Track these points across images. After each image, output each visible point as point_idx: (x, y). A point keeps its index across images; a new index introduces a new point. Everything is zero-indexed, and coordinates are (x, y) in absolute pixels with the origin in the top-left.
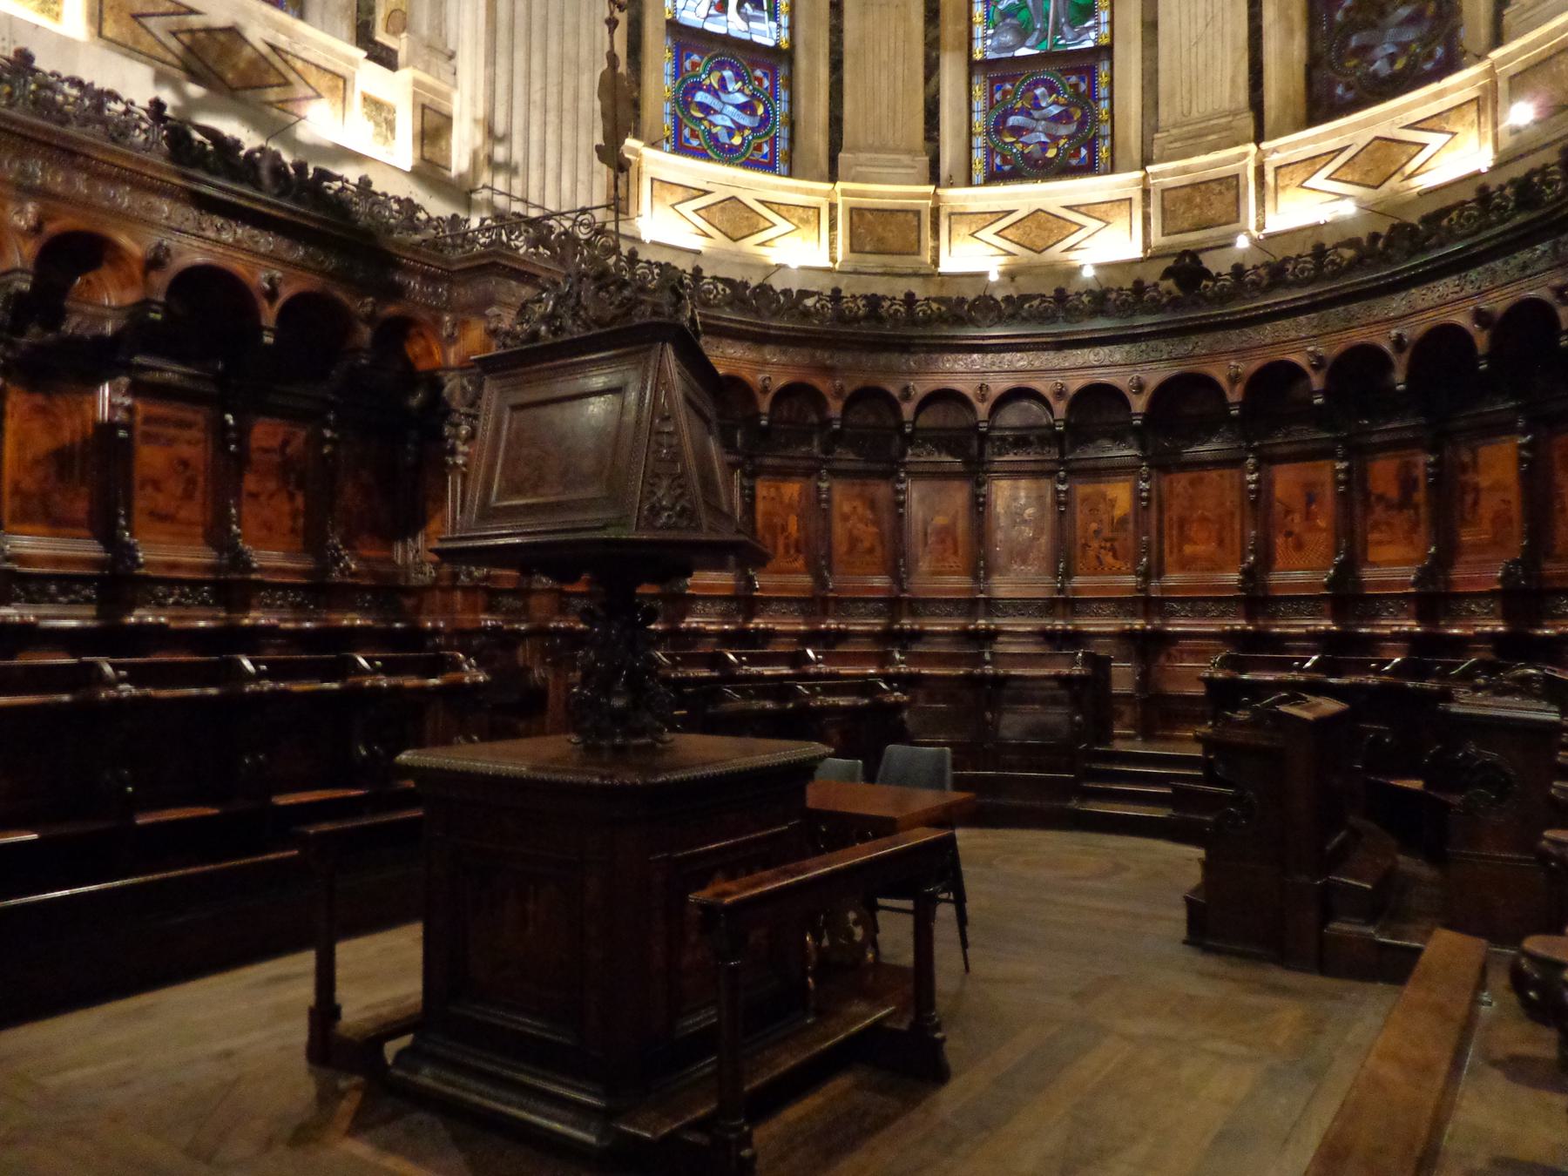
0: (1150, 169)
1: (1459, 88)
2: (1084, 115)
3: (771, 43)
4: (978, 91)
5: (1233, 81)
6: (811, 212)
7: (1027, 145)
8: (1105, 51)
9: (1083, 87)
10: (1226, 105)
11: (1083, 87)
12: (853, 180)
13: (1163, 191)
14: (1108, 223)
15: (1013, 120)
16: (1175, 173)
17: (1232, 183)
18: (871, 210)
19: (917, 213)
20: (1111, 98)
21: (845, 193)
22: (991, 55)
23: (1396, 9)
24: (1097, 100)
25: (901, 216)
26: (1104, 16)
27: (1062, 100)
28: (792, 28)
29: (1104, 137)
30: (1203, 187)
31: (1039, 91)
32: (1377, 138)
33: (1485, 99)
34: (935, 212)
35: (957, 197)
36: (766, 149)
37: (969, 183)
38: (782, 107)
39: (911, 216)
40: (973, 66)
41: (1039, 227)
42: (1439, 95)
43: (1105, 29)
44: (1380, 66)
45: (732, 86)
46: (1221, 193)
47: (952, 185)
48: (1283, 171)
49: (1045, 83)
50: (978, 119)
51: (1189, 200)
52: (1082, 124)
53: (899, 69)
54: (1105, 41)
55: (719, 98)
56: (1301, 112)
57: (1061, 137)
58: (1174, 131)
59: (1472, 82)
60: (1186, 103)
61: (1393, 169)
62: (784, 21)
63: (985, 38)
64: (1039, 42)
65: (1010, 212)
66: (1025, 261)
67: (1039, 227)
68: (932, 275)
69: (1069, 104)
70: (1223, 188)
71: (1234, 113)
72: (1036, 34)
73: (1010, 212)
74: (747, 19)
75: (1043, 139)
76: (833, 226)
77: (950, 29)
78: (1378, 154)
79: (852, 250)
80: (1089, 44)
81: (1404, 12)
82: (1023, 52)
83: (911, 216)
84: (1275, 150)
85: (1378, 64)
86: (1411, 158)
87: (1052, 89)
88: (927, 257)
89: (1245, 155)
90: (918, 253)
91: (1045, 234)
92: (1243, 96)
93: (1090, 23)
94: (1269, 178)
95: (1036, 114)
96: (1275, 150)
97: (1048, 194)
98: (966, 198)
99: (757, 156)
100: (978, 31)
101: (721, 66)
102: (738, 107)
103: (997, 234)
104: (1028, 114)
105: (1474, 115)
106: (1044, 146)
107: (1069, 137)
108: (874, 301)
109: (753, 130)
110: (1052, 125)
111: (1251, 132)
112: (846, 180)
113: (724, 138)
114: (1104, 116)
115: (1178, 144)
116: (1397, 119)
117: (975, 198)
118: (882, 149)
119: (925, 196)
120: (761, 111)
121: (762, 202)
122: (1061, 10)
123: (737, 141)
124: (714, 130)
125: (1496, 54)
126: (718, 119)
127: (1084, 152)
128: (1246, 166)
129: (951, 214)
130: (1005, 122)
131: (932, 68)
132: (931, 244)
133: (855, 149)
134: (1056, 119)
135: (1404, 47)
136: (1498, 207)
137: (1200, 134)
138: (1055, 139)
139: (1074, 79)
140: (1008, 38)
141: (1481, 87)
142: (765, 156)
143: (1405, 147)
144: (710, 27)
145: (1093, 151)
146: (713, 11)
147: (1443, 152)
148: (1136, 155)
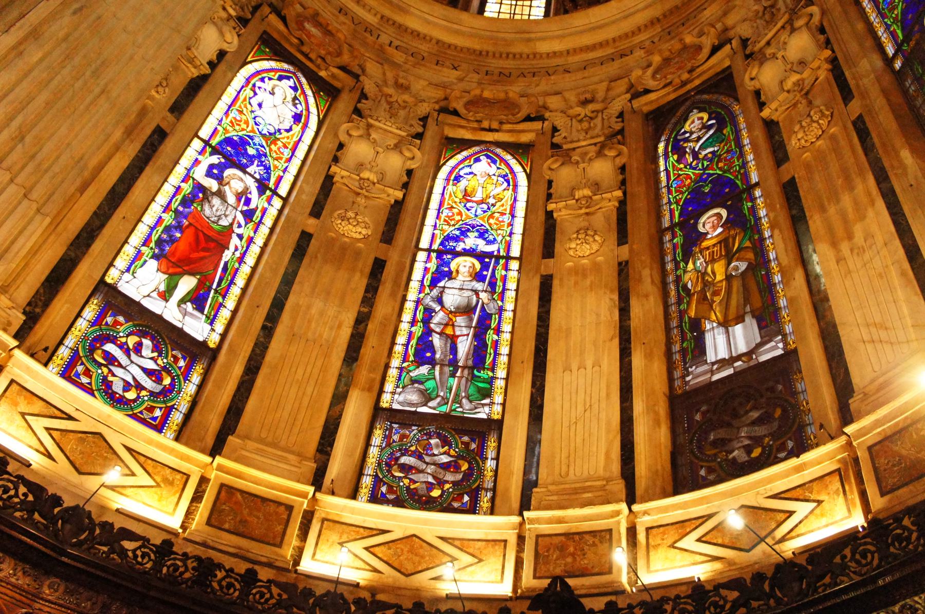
0: (526, 514)
1: (818, 462)
2: (471, 468)
3: (201, 339)
4: (378, 438)
5: (607, 455)
6: (179, 476)
7: (415, 482)
8: (495, 426)
9: (473, 446)
10: (601, 472)
12: (236, 460)
13: (538, 536)
14: (480, 560)
15: (405, 460)
16: (550, 521)
17: (605, 536)
18: (242, 492)
19: (290, 508)
20: (497, 459)
21: (220, 468)
22: (396, 406)
23: (747, 412)
25: (272, 507)
26: (498, 398)
27: (452, 452)
28: (223, 336)
29: (487, 490)
30: (577, 538)
33: (846, 470)
34: (308, 517)
35: (334, 505)
36: (158, 413)
37: (354, 495)
38: (190, 389)
39: (282, 508)
40: (378, 413)
42: (799, 469)
43: (498, 409)
44: (738, 454)
45: (147, 351)
46: (594, 544)
47: (333, 493)
48: (654, 531)
49: (439, 436)
50: (374, 452)
51: (562, 548)
52: (468, 475)
53: (309, 390)
55: (129, 356)
56: (670, 489)
57: (447, 482)
58: (551, 488)
59: (830, 456)
60: (564, 468)
62: (220, 326)
63: (393, 393)
64: (440, 405)
65: (384, 532)
66: (390, 581)
67: (411, 551)
68: (287, 570)
69: (459, 457)
70: (597, 541)
71: (608, 480)
72: (439, 399)
73: (384, 532)
74: (185, 314)
75: (431, 479)
76: (197, 497)
77: (364, 373)
79: (209, 523)
80: (483, 416)
81: (755, 415)
83: (282, 508)
84: (646, 513)
85: (736, 453)
86: (780, 524)
87: (445, 442)
88: (288, 552)
89: (618, 513)
90: (280, 545)
91: (417, 559)
92: (616, 467)
93: (487, 401)
94: (641, 536)
95: (427, 459)
96: (646, 513)
97: (426, 522)
98: (344, 508)
99: (146, 415)
100: (389, 387)
101: (143, 334)
102: (145, 370)
103: (367, 549)
104: (420, 457)
105: (838, 485)
106: (430, 487)
107: (454, 483)
108: (206, 567)
109: (152, 393)
110: (440, 470)
111: (623, 495)
112: (228, 458)
113: (118, 387)
114: (489, 474)
115: (555, 498)
116: (761, 490)
117: (353, 511)
118: (274, 445)
119: (304, 495)
120: (167, 381)
121: (129, 450)
122: (463, 388)
123: (131, 395)
124: (110, 378)
125: (849, 430)
126: (118, 371)
127: (466, 498)
128: (619, 523)
129: (324, 520)
131: (339, 398)
132: (295, 542)
133: (247, 437)
134: (445, 467)
135: (757, 441)
136: (899, 538)
137: (576, 491)
138: (441, 483)
139: (466, 439)
140: (414, 397)
141: (839, 461)
142: (155, 419)
143: (772, 514)
144: (146, 303)
145: (475, 500)
146: (155, 294)
147: (812, 517)
148: (515, 502)
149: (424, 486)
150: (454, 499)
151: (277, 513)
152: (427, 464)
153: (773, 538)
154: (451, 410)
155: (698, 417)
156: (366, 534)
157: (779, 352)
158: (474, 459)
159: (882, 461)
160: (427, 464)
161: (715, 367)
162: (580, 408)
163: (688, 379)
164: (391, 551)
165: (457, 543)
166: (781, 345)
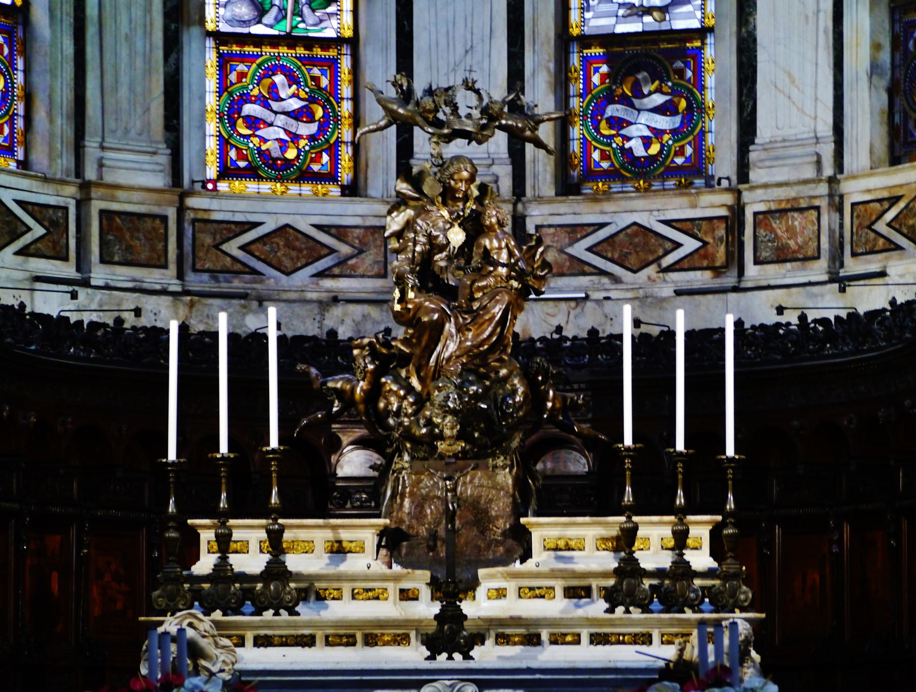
2: (326, 115)
9: (325, 82)
11: (325, 82)
15: (249, 109)
22: (224, 28)
23: (650, 93)
24: (339, 100)
27: (302, 95)
31: (279, 79)
32: (635, 224)
39: (158, 222)
41: (289, 245)
43: (348, 19)
54: (348, 33)
57: (301, 137)
61: (651, 258)
64: (278, 20)
72: (274, 11)
78: (637, 240)
80: (330, 33)
81: (658, 99)
82: (258, 30)
86: (667, 253)
87: (292, 79)
91: (294, 254)
95: (275, 105)
104: (267, 106)
107: (312, 138)
127: (325, 158)
130: (240, 110)
131: (173, 45)
134: (295, 115)
138: (295, 138)
139: (316, 71)
140: (244, 11)
149: (277, 145)
150: (313, 160)
151: (154, 228)
152: (276, 113)
153: (659, 266)
154: (293, 28)
155: (596, 79)
156: (238, 230)
157: (695, 24)
158: (328, 100)
159: (762, 232)
160: (276, 113)
161: (621, 12)
162: (460, 50)
163: (588, 15)
164: (267, 248)
165: (333, 231)
166: (699, 14)
